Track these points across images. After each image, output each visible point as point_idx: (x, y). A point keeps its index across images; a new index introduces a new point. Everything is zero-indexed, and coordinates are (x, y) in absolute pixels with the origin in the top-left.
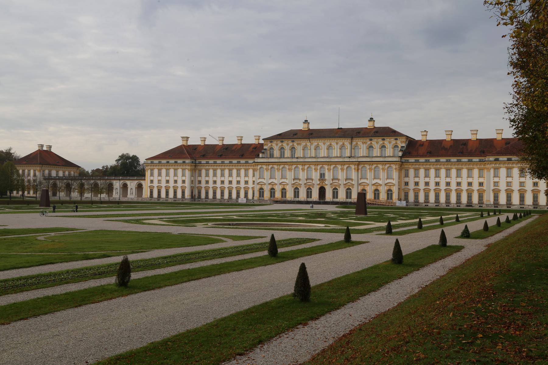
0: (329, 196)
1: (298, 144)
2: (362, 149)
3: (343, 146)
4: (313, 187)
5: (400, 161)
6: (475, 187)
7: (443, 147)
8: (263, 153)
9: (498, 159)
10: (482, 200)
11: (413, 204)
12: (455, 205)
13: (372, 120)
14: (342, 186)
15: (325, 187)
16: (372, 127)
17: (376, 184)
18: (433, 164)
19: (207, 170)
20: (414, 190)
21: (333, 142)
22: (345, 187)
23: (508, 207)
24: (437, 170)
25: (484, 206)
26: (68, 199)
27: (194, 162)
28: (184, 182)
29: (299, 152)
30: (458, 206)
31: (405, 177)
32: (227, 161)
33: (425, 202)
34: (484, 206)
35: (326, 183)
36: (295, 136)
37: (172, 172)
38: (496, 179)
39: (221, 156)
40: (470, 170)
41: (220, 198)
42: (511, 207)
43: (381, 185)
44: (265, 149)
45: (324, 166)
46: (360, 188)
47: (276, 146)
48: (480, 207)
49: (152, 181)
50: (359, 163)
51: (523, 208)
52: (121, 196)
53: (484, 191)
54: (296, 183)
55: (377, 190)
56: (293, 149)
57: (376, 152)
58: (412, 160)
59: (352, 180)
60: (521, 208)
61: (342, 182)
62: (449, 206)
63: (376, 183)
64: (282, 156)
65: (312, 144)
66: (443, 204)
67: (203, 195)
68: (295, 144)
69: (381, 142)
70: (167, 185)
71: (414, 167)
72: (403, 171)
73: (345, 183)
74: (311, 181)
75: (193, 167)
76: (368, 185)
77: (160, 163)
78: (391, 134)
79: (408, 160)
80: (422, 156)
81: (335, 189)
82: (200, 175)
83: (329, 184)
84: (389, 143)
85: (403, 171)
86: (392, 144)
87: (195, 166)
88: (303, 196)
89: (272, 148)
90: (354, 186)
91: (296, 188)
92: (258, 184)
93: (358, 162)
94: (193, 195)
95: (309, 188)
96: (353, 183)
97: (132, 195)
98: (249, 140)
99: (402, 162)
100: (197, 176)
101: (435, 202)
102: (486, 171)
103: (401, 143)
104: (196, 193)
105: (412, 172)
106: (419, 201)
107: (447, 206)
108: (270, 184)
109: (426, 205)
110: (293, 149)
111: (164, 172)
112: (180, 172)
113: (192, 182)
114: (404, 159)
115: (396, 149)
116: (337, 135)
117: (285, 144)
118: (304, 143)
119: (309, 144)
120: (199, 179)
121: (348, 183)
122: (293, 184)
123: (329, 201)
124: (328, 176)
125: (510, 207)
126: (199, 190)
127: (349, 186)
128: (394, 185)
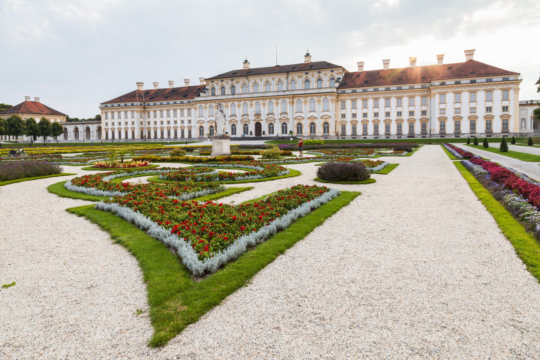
1: (237, 82)
2: (298, 84)
3: (280, 81)
4: (249, 123)
7: (381, 76)
8: (205, 92)
9: (445, 83)
10: (426, 130)
11: (350, 137)
12: (395, 136)
14: (277, 121)
15: (261, 122)
17: (312, 117)
18: (371, 93)
19: (155, 112)
20: (351, 122)
21: (270, 78)
22: (280, 122)
24: (376, 99)
25: (427, 136)
26: (56, 142)
27: (143, 104)
28: (133, 123)
29: (239, 89)
32: (172, 102)
33: (363, 135)
34: (427, 136)
35: (262, 118)
37: (123, 114)
38: (443, 106)
39: (167, 97)
40: (411, 97)
41: (167, 138)
43: (316, 118)
44: (207, 89)
46: (296, 122)
47: (217, 85)
49: (107, 124)
50: (294, 96)
52: (85, 139)
53: (427, 120)
54: (233, 119)
55: (313, 124)
56: (233, 87)
57: (313, 84)
58: (349, 91)
59: (286, 113)
61: (277, 116)
62: (389, 138)
63: (312, 116)
64: (223, 94)
65: (249, 81)
67: (152, 136)
68: (234, 82)
69: (316, 74)
70: (120, 126)
71: (351, 98)
72: (340, 103)
73: (280, 117)
74: (246, 117)
75: (142, 109)
76: (303, 118)
77: (112, 106)
79: (344, 91)
80: (360, 86)
81: (271, 124)
82: (149, 117)
83: (264, 120)
84: (326, 75)
85: (340, 103)
87: (144, 108)
88: (240, 132)
89: (213, 88)
90: (289, 120)
91: (234, 125)
92: (198, 122)
94: (144, 136)
95: (246, 125)
96: (288, 117)
97: (94, 138)
98: (195, 82)
99: (339, 94)
100: (146, 117)
101: (374, 135)
104: (146, 133)
105: (348, 103)
106: (356, 133)
107: (386, 138)
109: (364, 138)
110: (233, 87)
111: (116, 114)
112: (129, 113)
113: (141, 123)
114: (340, 91)
115: (333, 81)
116: (274, 71)
117: (224, 83)
118: (242, 80)
119: (246, 81)
120: (149, 120)
121: (284, 117)
122: (230, 121)
124: (264, 111)
126: (148, 131)
128: (330, 117)
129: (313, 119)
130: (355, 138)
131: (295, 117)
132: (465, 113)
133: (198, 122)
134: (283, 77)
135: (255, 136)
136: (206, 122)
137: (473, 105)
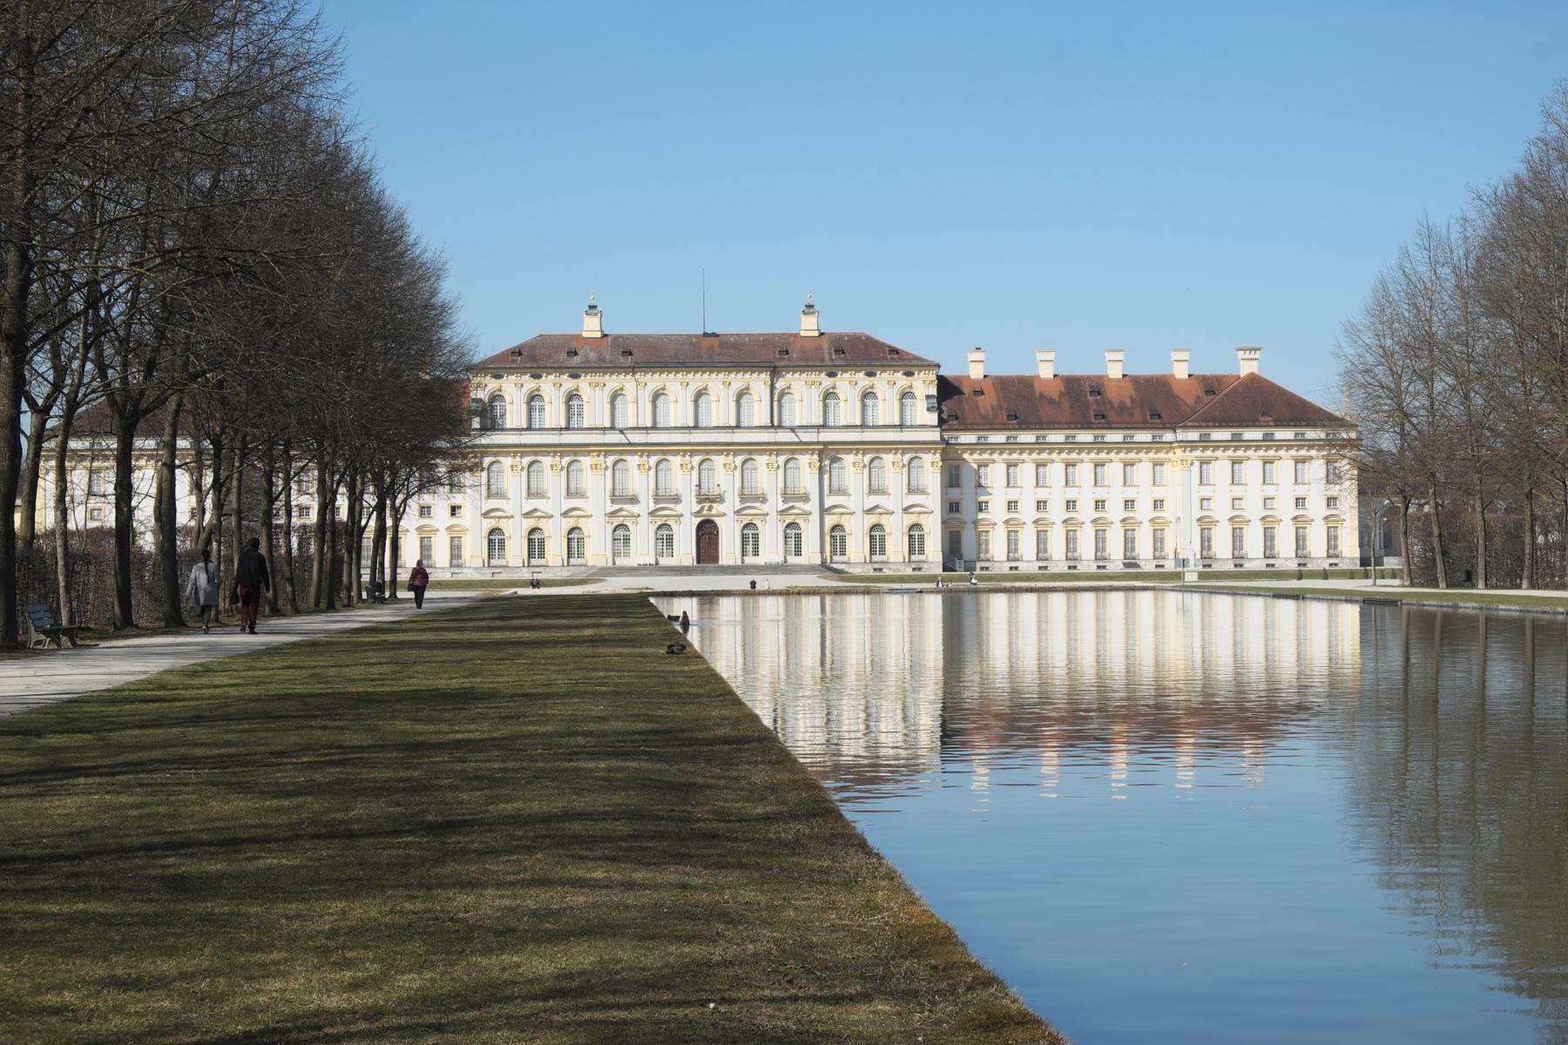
0: (729, 550)
5: (939, 439)
6: (1144, 511)
13: (811, 310)
15: (716, 520)
16: (816, 334)
17: (880, 510)
23: (1236, 566)
30: (1099, 567)
31: (951, 486)
36: (577, 360)
38: (1206, 491)
42: (1245, 566)
45: (713, 457)
46: (830, 521)
48: (1157, 566)
51: (1273, 565)
55: (876, 527)
57: (847, 411)
60: (1268, 565)
66: (1059, 563)
73: (782, 507)
78: (889, 357)
83: (730, 514)
84: (887, 384)
86: (897, 387)
92: (486, 515)
93: (818, 443)
102: (1167, 466)
103: (924, 385)
108: (528, 515)
109: (1011, 568)
122: (613, 514)
123: (732, 563)
125: (1241, 566)
127: (793, 517)
129: (881, 514)
130: (987, 568)
131: (826, 506)
132: (1253, 510)
133: (486, 515)
134: (758, 383)
135: (695, 564)
136: (518, 516)
137: (1269, 491)
